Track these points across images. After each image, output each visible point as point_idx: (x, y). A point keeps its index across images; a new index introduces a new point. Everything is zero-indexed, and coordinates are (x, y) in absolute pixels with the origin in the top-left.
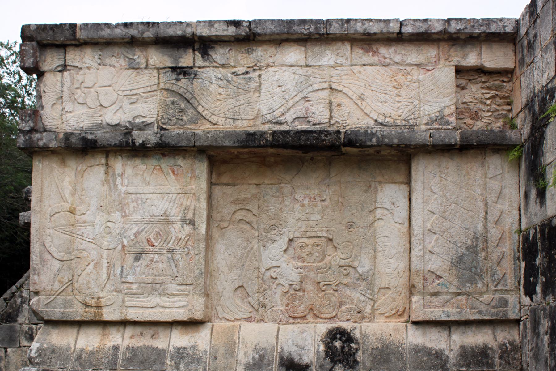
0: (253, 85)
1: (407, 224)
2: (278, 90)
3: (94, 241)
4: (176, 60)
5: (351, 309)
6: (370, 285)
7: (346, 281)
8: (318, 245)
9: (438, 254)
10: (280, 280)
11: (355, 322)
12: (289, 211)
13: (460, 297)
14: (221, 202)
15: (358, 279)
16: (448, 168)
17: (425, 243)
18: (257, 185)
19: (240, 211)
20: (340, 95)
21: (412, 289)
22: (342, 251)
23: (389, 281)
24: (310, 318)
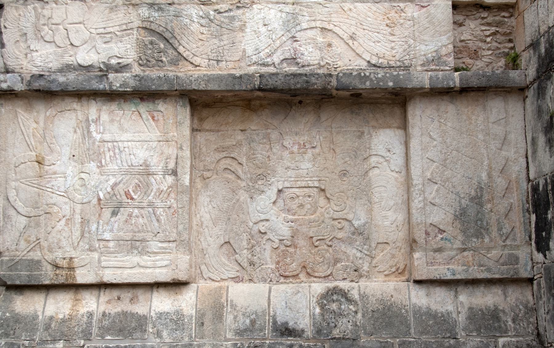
1: (404, 172)
2: (263, 29)
3: (66, 194)
5: (347, 267)
7: (340, 235)
8: (309, 196)
9: (440, 206)
10: (270, 235)
11: (352, 281)
12: (278, 159)
13: (465, 253)
14: (204, 149)
15: (353, 234)
16: (447, 112)
17: (426, 194)
18: (242, 131)
19: (224, 160)
20: (330, 34)
21: (412, 244)
22: (335, 202)
23: (387, 235)
24: (302, 276)
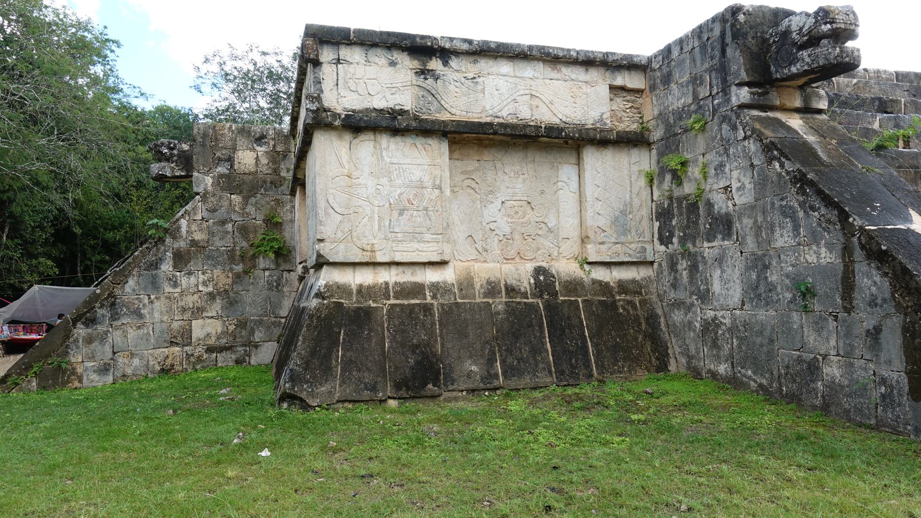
0: (479, 88)
1: (578, 193)
2: (496, 93)
3: (367, 200)
4: (424, 64)
6: (557, 236)
10: (497, 232)
20: (537, 99)
24: (517, 259)
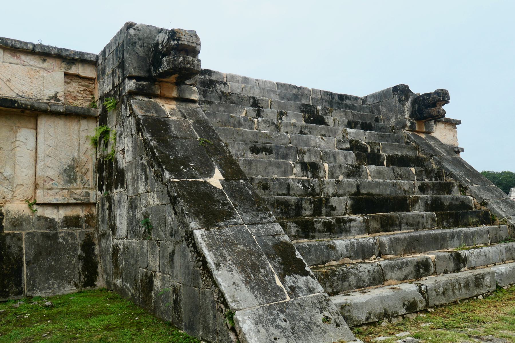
1: (34, 150)
6: (11, 183)
9: (52, 168)
13: (64, 191)
15: (3, 179)
21: (36, 186)
